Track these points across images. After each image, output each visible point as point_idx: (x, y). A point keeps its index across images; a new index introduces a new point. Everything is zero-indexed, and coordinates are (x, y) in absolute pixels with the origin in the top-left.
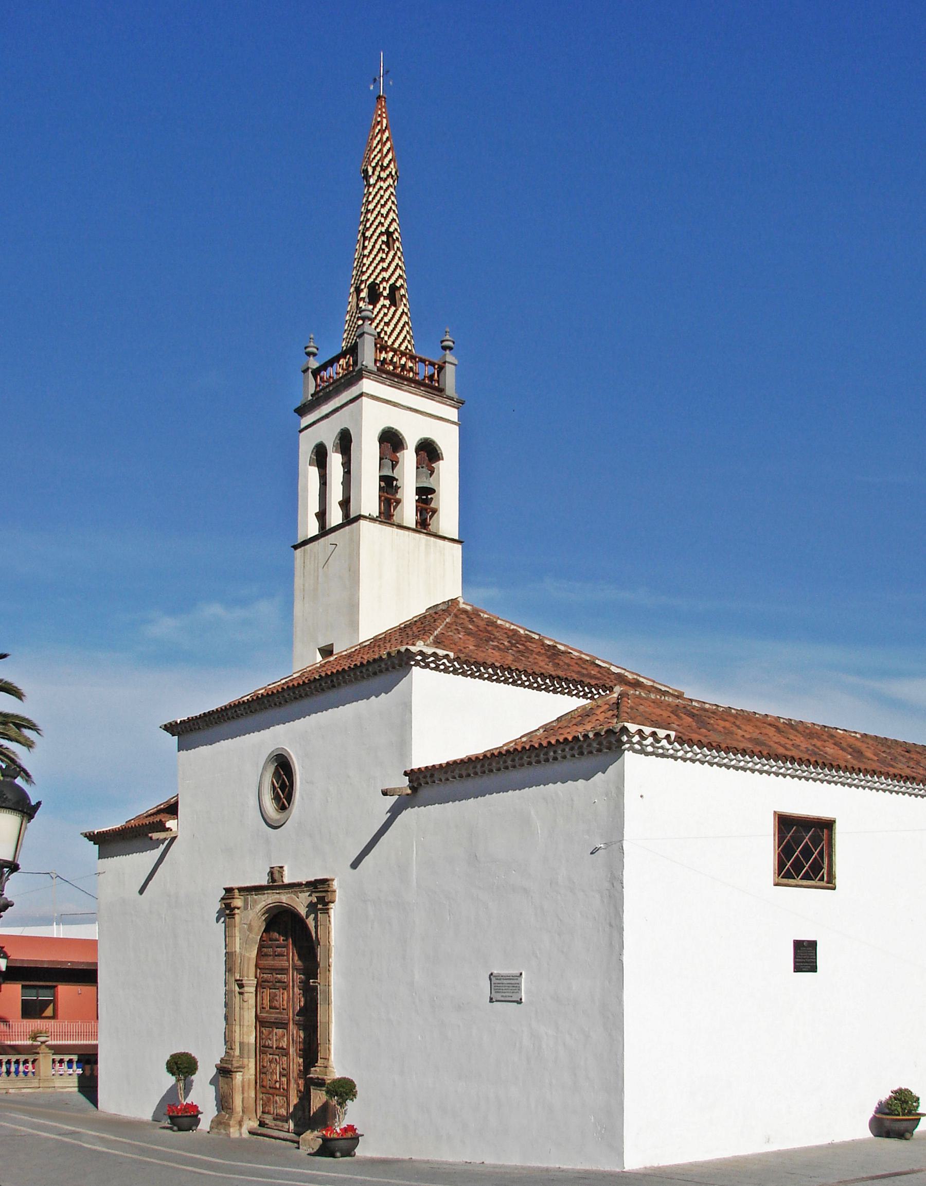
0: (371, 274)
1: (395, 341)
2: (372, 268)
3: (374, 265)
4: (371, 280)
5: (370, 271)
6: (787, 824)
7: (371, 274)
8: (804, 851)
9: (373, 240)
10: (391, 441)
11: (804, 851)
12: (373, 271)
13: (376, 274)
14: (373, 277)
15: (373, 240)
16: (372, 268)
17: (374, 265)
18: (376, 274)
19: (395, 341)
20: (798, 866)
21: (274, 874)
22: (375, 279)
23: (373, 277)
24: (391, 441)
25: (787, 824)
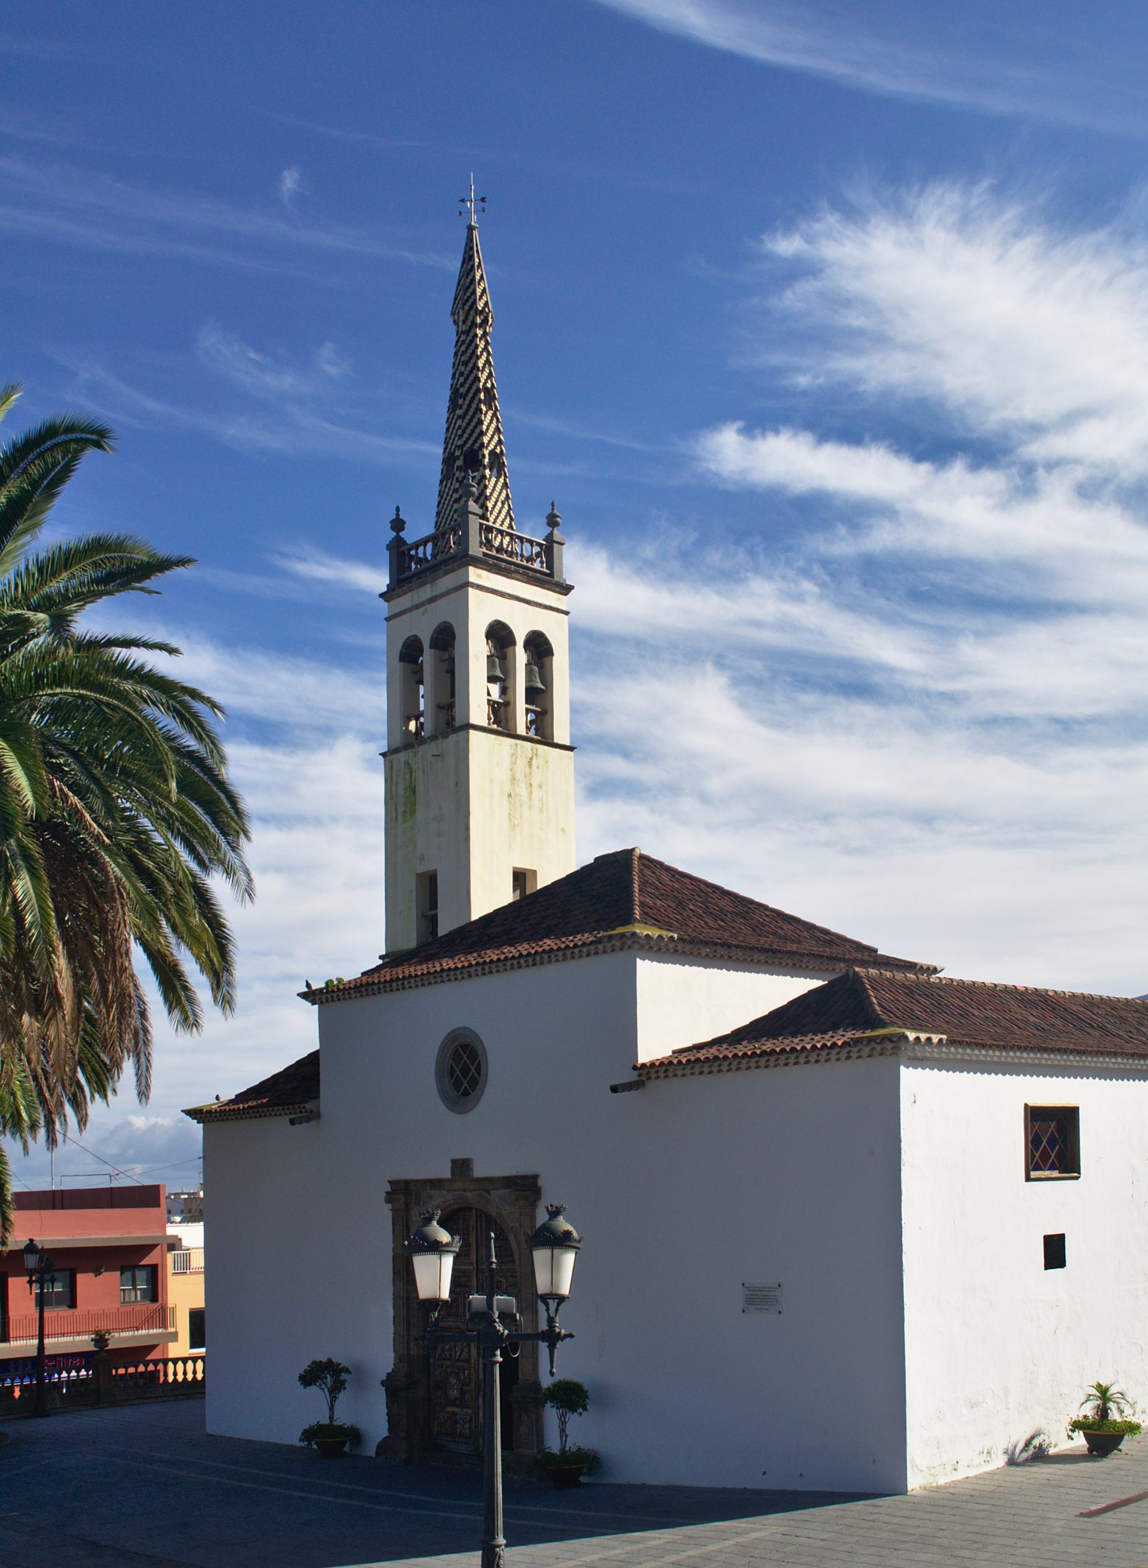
0: (468, 439)
1: (497, 517)
2: (468, 431)
3: (471, 427)
4: (468, 445)
5: (466, 435)
6: (1036, 1116)
7: (468, 439)
8: (1053, 1143)
9: (468, 399)
10: (499, 635)
11: (1053, 1143)
12: (470, 435)
13: (473, 438)
14: (470, 442)
15: (468, 399)
16: (468, 431)
17: (471, 427)
18: (473, 438)
19: (497, 517)
20: (1045, 1156)
21: (461, 1167)
22: (473, 444)
23: (470, 442)
24: (499, 635)
25: (1036, 1116)
